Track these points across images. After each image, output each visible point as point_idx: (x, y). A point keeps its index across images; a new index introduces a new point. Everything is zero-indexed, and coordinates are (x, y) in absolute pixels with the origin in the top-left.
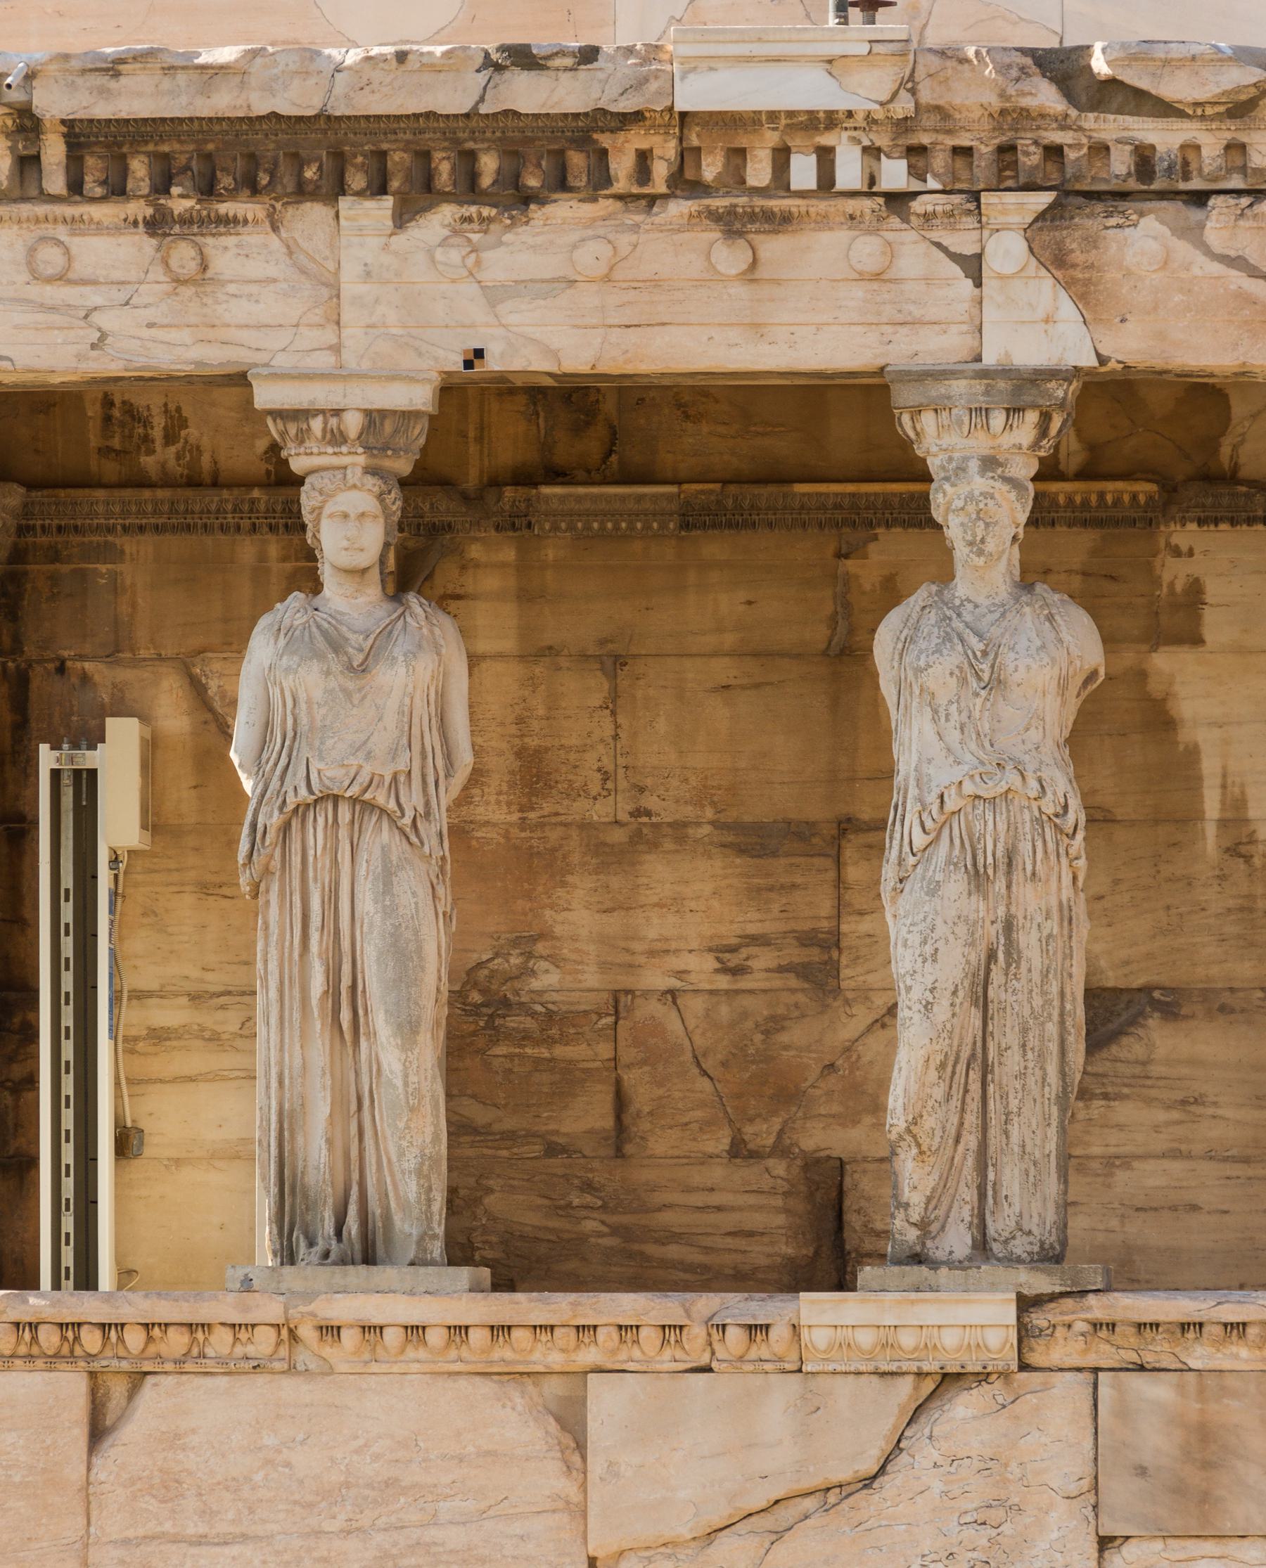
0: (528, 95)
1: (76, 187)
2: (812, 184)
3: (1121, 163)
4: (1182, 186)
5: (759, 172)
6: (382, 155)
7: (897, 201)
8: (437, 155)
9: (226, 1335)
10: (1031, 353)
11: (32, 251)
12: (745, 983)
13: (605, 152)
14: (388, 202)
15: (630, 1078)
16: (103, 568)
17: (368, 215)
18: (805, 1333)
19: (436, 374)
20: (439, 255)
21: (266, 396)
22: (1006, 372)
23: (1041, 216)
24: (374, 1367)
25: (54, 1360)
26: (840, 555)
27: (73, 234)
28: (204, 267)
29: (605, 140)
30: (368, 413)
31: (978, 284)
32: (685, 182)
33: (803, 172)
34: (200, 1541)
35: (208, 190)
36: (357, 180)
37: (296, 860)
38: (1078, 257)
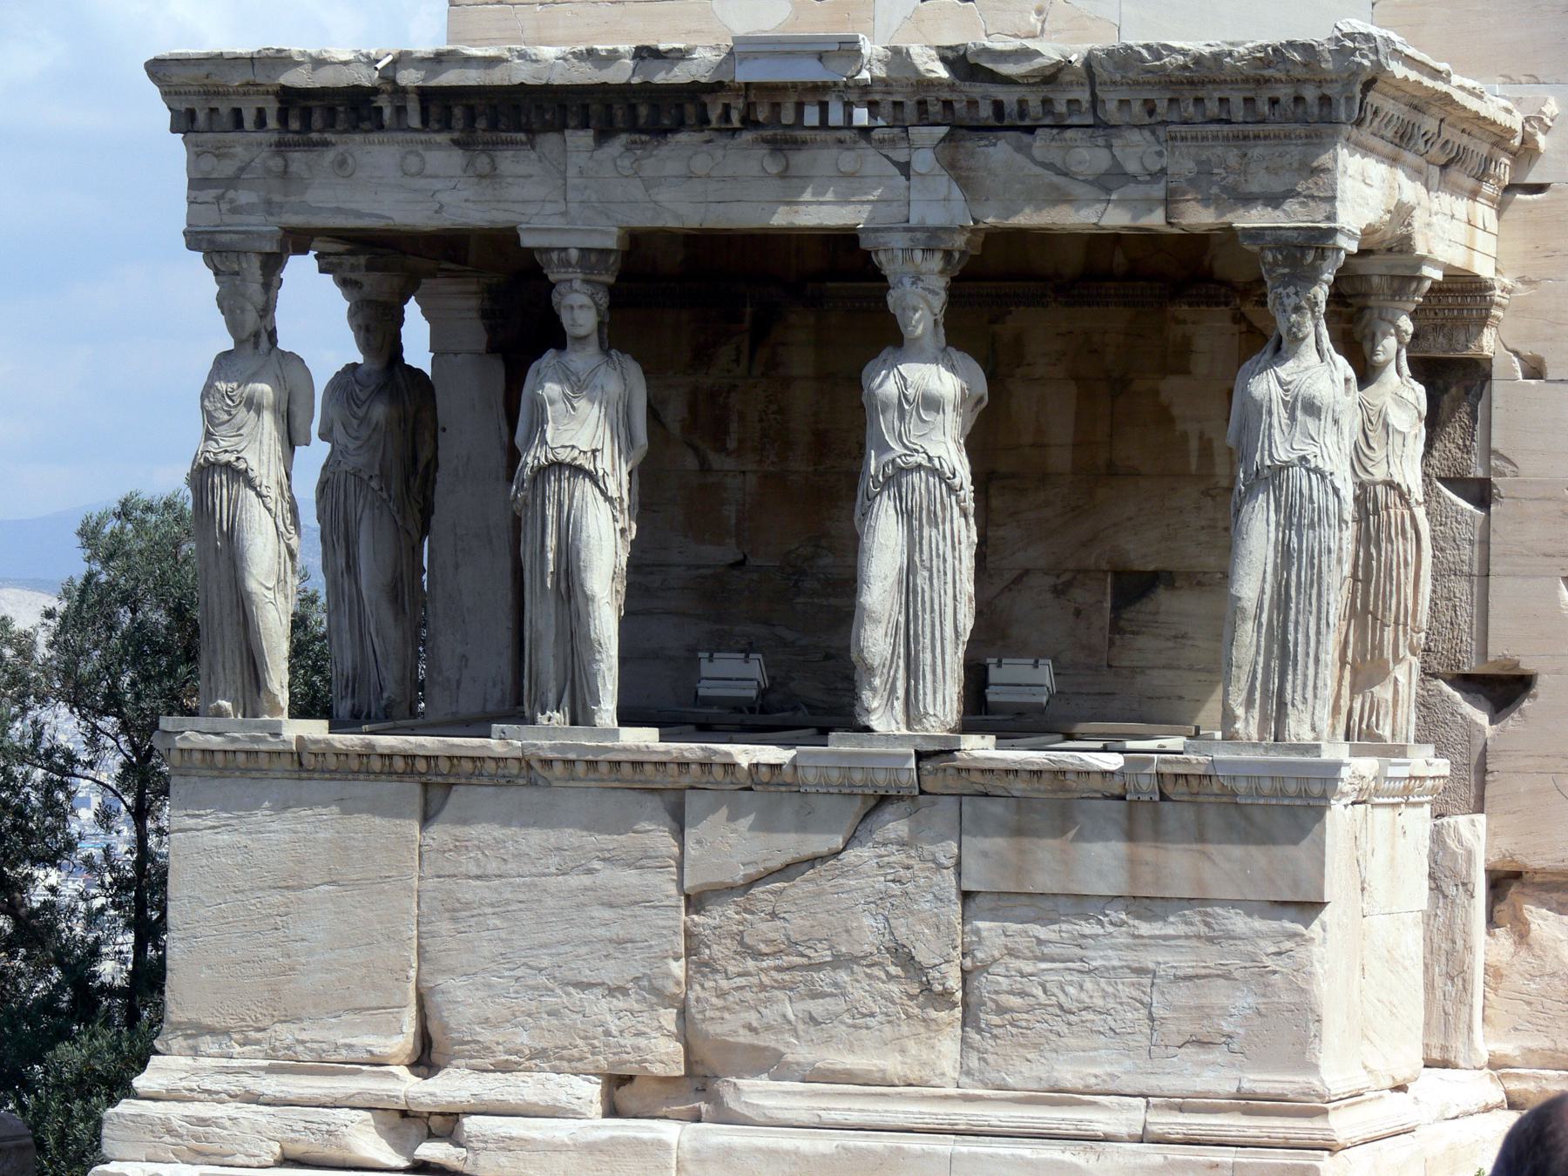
1: (425, 121)
2: (816, 123)
3: (985, 112)
5: (788, 117)
6: (586, 107)
7: (865, 131)
9: (492, 764)
10: (934, 216)
11: (403, 158)
13: (704, 106)
14: (591, 132)
17: (580, 140)
18: (800, 771)
19: (615, 229)
20: (619, 162)
21: (527, 241)
23: (943, 140)
24: (572, 784)
25: (401, 776)
26: (992, 322)
29: (707, 99)
30: (581, 250)
31: (908, 179)
32: (749, 122)
33: (812, 116)
34: (478, 877)
35: (493, 126)
37: (539, 501)
38: (963, 163)
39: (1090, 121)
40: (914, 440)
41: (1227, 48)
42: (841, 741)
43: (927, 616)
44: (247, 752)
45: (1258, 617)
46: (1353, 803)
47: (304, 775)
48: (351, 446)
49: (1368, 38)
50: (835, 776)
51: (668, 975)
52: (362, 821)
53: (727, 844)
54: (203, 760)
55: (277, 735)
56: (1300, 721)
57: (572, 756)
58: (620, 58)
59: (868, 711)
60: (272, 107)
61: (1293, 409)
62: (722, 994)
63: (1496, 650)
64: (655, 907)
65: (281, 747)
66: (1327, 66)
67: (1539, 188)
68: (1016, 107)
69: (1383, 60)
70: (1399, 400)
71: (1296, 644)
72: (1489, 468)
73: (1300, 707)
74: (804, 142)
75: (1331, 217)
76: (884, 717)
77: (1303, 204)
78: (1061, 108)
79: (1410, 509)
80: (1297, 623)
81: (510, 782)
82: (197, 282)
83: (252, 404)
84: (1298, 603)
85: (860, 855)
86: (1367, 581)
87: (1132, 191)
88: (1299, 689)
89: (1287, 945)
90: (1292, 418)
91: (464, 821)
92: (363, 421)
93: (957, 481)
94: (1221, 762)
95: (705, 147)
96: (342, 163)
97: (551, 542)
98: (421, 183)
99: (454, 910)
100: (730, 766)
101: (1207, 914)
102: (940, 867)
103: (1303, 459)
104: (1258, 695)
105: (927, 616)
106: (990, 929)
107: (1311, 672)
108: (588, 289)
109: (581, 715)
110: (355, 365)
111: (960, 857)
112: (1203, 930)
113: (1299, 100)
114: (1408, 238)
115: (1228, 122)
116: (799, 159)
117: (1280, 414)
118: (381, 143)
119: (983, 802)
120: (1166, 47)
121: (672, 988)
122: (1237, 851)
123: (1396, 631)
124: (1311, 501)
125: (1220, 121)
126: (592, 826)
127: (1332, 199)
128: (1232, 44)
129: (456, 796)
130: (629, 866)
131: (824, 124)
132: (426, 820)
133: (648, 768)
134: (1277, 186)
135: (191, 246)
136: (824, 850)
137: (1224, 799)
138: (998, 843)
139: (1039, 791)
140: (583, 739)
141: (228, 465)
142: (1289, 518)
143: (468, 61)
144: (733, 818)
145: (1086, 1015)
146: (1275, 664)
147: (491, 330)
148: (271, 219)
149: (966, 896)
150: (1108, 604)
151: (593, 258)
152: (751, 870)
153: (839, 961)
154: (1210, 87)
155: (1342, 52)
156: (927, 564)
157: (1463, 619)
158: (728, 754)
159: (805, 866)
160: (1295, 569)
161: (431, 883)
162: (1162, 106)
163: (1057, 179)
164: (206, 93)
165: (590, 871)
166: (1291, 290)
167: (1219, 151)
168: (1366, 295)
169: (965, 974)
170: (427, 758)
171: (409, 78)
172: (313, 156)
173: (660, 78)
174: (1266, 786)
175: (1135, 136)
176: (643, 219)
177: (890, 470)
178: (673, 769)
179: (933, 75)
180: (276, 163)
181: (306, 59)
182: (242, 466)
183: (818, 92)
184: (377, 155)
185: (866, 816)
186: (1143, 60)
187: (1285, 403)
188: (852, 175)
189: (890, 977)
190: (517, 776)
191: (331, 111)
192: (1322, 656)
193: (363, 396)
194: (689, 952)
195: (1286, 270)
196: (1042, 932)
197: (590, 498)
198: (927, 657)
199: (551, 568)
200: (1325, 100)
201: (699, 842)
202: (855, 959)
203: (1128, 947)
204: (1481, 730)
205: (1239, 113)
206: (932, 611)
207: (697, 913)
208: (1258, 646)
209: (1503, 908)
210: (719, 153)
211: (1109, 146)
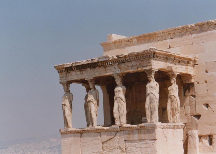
3: (121, 61)
5: (105, 64)
7: (111, 65)
21: (86, 80)
32: (102, 65)
33: (107, 64)
49: (152, 48)
51: (101, 151)
52: (75, 138)
53: (105, 137)
59: (116, 123)
60: (65, 70)
62: (105, 153)
63: (197, 112)
67: (197, 64)
70: (174, 87)
75: (151, 67)
76: (117, 123)
78: (127, 60)
82: (61, 86)
86: (172, 106)
87: (134, 67)
89: (153, 144)
91: (84, 137)
93: (122, 99)
97: (89, 108)
100: (104, 129)
103: (151, 92)
107: (154, 115)
112: (145, 143)
113: (147, 56)
114: (172, 70)
116: (106, 68)
117: (149, 88)
121: (101, 152)
122: (148, 134)
125: (141, 59)
127: (151, 65)
129: (83, 135)
131: (108, 65)
132: (81, 137)
134: (147, 65)
138: (127, 135)
140: (92, 128)
143: (78, 63)
144: (105, 135)
145: (136, 152)
146: (151, 114)
147: (107, 90)
149: (125, 141)
150: (162, 111)
152: (107, 140)
153: (115, 148)
157: (194, 110)
162: (135, 58)
163: (128, 67)
165: (94, 141)
169: (126, 149)
171: (74, 65)
175: (134, 62)
176: (94, 76)
178: (100, 130)
180: (66, 75)
183: (107, 61)
189: (119, 150)
191: (69, 69)
194: (103, 148)
196: (132, 144)
198: (121, 117)
200: (149, 55)
202: (116, 148)
203: (140, 145)
205: (142, 58)
209: (201, 139)
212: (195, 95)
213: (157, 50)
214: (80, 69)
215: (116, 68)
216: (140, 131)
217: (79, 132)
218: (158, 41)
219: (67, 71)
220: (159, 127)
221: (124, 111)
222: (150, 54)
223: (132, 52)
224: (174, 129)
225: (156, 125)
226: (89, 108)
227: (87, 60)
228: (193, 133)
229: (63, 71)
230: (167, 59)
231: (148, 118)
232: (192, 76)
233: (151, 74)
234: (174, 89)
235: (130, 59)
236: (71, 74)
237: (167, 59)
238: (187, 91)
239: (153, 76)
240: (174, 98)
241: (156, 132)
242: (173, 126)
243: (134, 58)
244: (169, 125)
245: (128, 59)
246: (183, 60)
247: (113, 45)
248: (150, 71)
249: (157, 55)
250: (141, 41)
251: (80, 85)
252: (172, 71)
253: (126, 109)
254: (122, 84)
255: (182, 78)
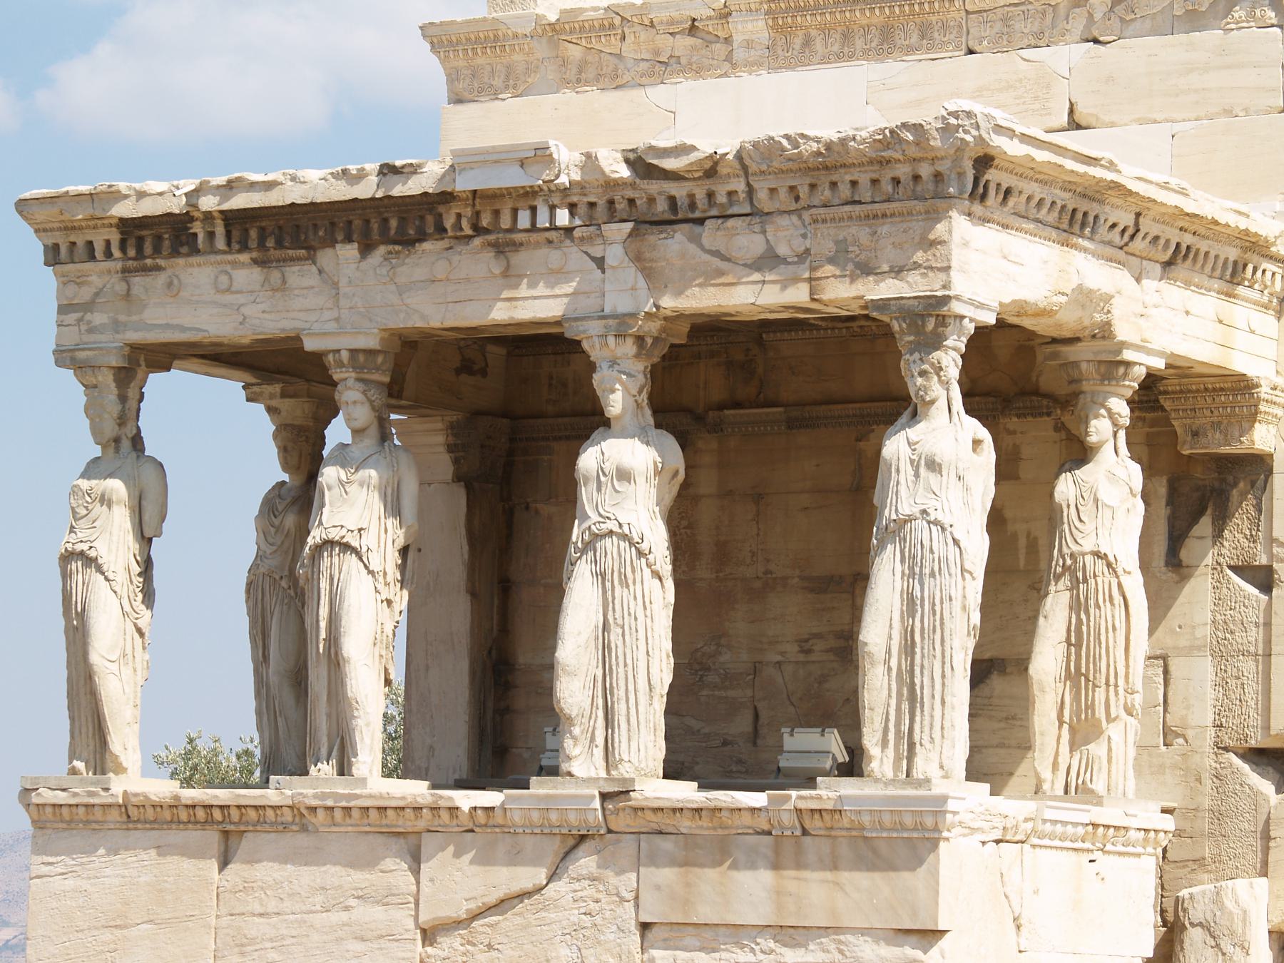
0: (401, 189)
1: (229, 244)
3: (662, 206)
4: (691, 216)
5: (505, 222)
6: (350, 222)
7: (568, 231)
8: (373, 220)
12: (813, 657)
13: (440, 215)
14: (356, 245)
15: (760, 706)
16: (546, 458)
17: (349, 252)
18: (508, 813)
19: (376, 331)
21: (310, 345)
22: (614, 316)
23: (630, 235)
26: (858, 440)
27: (233, 269)
28: (284, 282)
29: (441, 209)
30: (351, 351)
31: (603, 272)
32: (478, 230)
33: (524, 220)
34: (261, 915)
36: (340, 237)
38: (647, 255)
39: (747, 210)
40: (607, 509)
41: (851, 133)
42: (541, 785)
43: (621, 670)
44: (86, 806)
45: (887, 662)
46: (998, 842)
47: (131, 826)
48: (268, 552)
49: (969, 114)
50: (535, 816)
53: (455, 880)
54: (54, 814)
55: (107, 789)
56: (927, 759)
57: (330, 803)
58: (367, 175)
59: (569, 758)
60: (115, 237)
61: (918, 467)
64: (397, 940)
65: (110, 800)
66: (936, 143)
68: (686, 202)
69: (985, 136)
70: (1111, 475)
71: (922, 688)
72: (1271, 556)
73: (928, 745)
74: (521, 244)
76: (583, 762)
77: (923, 275)
78: (721, 198)
79: (1117, 577)
80: (922, 667)
81: (285, 827)
83: (106, 500)
84: (923, 648)
85: (560, 888)
86: (1078, 645)
88: (927, 729)
90: (917, 475)
92: (278, 529)
93: (644, 547)
94: (848, 797)
95: (446, 254)
96: (170, 285)
97: (324, 612)
98: (228, 298)
99: (242, 945)
100: (454, 810)
101: (840, 942)
102: (622, 900)
103: (924, 512)
104: (891, 736)
105: (621, 670)
106: (663, 958)
108: (360, 386)
109: (344, 769)
110: (283, 483)
111: (638, 889)
113: (917, 178)
114: (1109, 324)
115: (860, 202)
116: (519, 258)
117: (907, 471)
118: (199, 265)
119: (658, 839)
120: (802, 136)
123: (1108, 691)
124: (931, 551)
126: (352, 865)
127: (947, 269)
128: (857, 129)
129: (247, 843)
130: (378, 903)
131: (533, 228)
133: (390, 812)
135: (59, 363)
136: (528, 885)
137: (854, 833)
138: (667, 875)
139: (702, 827)
140: (341, 787)
141: (82, 554)
142: (911, 568)
143: (253, 186)
144: (457, 855)
146: (905, 706)
147: (456, 461)
148: (117, 336)
149: (645, 927)
151: (361, 358)
152: (472, 905)
154: (842, 171)
155: (947, 130)
156: (620, 621)
157: (1250, 697)
158: (451, 798)
159: (516, 901)
160: (918, 616)
161: (226, 921)
162: (803, 191)
164: (66, 228)
165: (347, 908)
166: (917, 356)
167: (854, 230)
168: (1079, 381)
170: (221, 807)
171: (208, 203)
172: (148, 279)
173: (399, 190)
174: (887, 819)
175: (784, 221)
177: (586, 537)
179: (616, 176)
180: (121, 287)
181: (132, 192)
182: (92, 553)
183: (528, 195)
184: (197, 275)
185: (567, 854)
186: (784, 149)
187: (912, 461)
188: (559, 271)
190: (293, 823)
191: (158, 239)
192: (948, 699)
193: (280, 508)
195: (912, 338)
197: (354, 572)
198: (620, 708)
199: (323, 635)
200: (938, 176)
201: (432, 880)
204: (1267, 800)
205: (865, 193)
206: (626, 665)
207: (431, 945)
208: (890, 689)
210: (458, 257)
211: (764, 232)
212: (1269, 570)
213: (1010, 133)
214: (262, 245)
215: (609, 261)
216: (786, 847)
217: (209, 822)
218: (971, 52)
219: (140, 249)
220: (973, 830)
221: (653, 660)
222: (943, 167)
223: (777, 133)
224: (1086, 857)
225: (951, 805)
226: (324, 612)
227: (345, 172)
228: (1229, 904)
229: (99, 253)
230: (1077, 228)
231: (879, 735)
232: (1264, 391)
233: (936, 342)
234: (1109, 494)
235: (751, 191)
236: (170, 285)
237: (1077, 228)
238: (1205, 525)
239: (950, 360)
240: (1105, 579)
241: (942, 871)
242: (1081, 830)
243: (792, 188)
244: (1049, 814)
245: (731, 194)
246: (1203, 246)
247: (541, 50)
248: (930, 316)
249: (1007, 181)
250: (807, 42)
251: (227, 390)
252: (1104, 332)
253: (668, 645)
254: (648, 412)
255: (1167, 405)
